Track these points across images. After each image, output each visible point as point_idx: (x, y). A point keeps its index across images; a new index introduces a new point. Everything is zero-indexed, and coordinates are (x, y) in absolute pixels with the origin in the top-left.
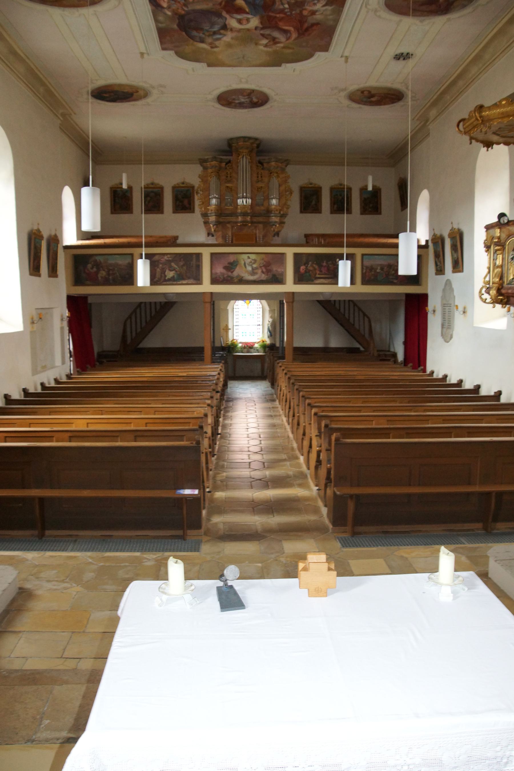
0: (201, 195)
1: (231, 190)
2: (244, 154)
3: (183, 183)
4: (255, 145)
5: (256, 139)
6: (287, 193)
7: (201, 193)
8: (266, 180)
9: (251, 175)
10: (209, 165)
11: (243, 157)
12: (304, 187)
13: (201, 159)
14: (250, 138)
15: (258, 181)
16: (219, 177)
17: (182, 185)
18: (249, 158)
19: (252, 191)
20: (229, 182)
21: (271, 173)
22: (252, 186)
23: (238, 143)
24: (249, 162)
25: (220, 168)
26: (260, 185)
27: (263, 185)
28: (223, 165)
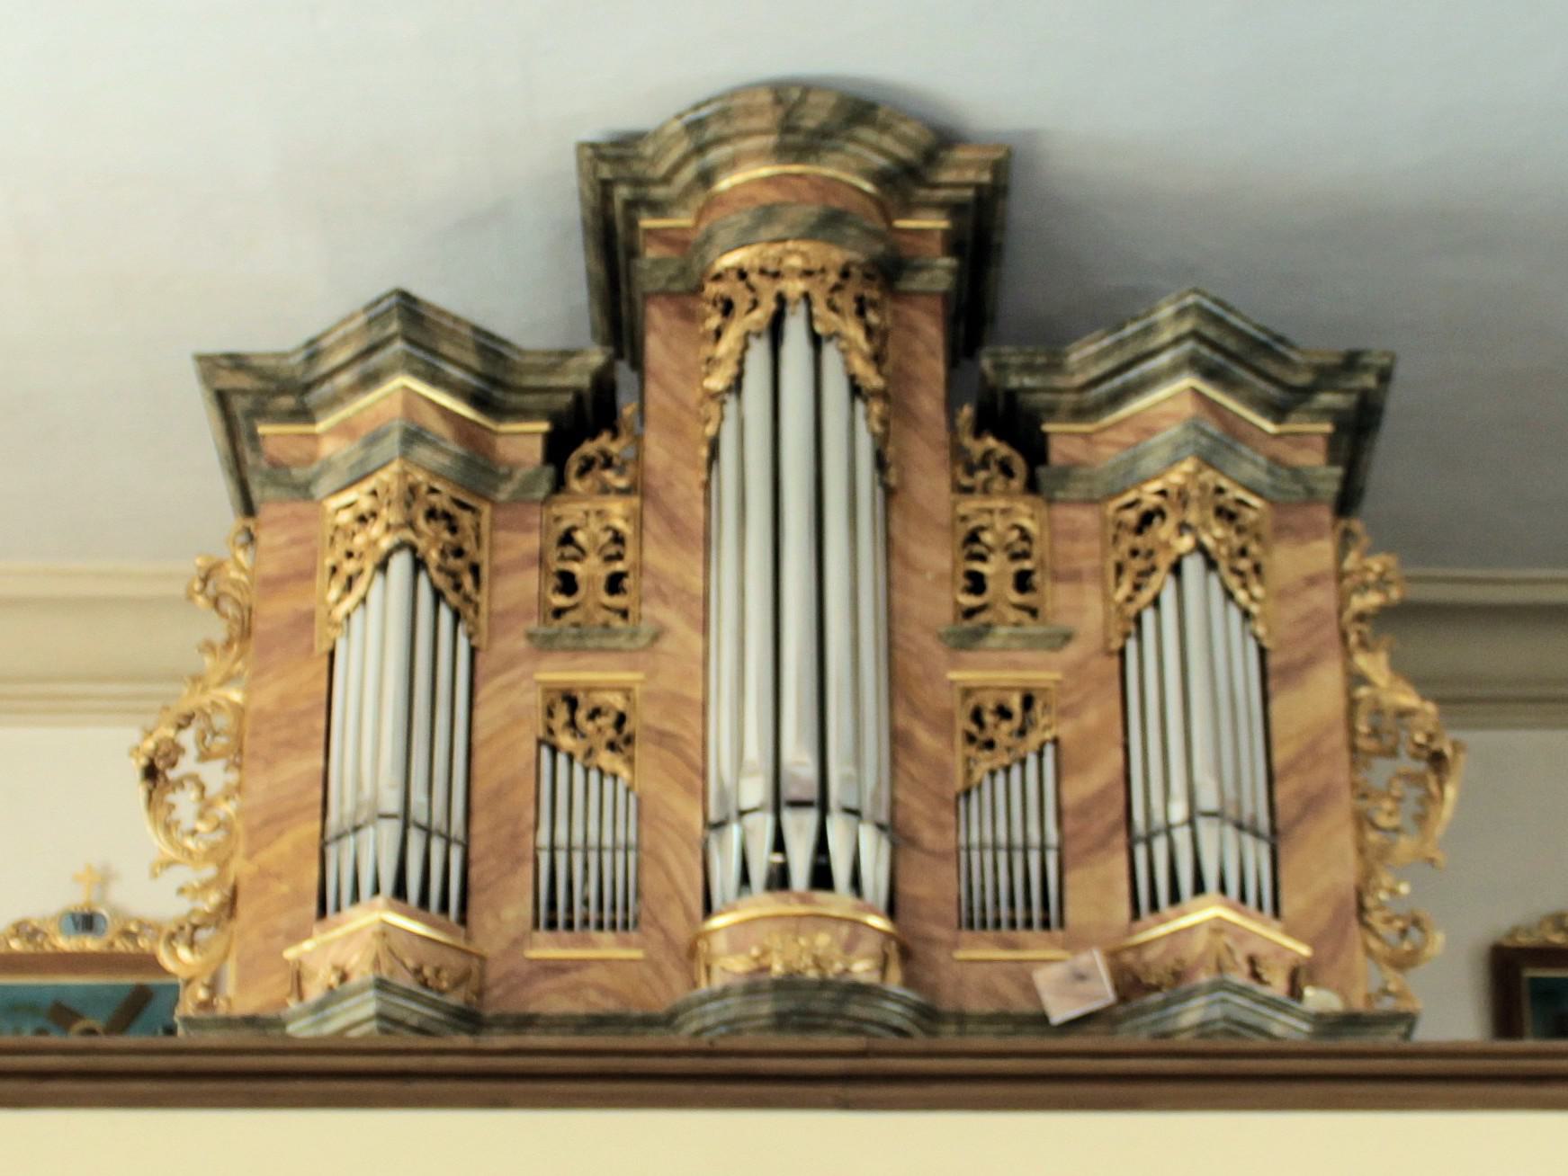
0: (206, 806)
1: (622, 741)
2: (794, 287)
3: (87, 922)
4: (935, 223)
5: (943, 141)
6: (1381, 772)
7: (216, 775)
8: (1084, 608)
9: (890, 547)
10: (329, 447)
11: (775, 331)
12: (1543, 955)
13: (237, 362)
14: (859, 111)
15: (970, 631)
16: (454, 581)
17: (66, 943)
18: (854, 331)
19: (898, 741)
20: (581, 643)
21: (1147, 519)
22: (898, 683)
23: (706, 178)
24: (856, 390)
25: (479, 469)
26: (993, 671)
27: (1041, 671)
28: (522, 441)
